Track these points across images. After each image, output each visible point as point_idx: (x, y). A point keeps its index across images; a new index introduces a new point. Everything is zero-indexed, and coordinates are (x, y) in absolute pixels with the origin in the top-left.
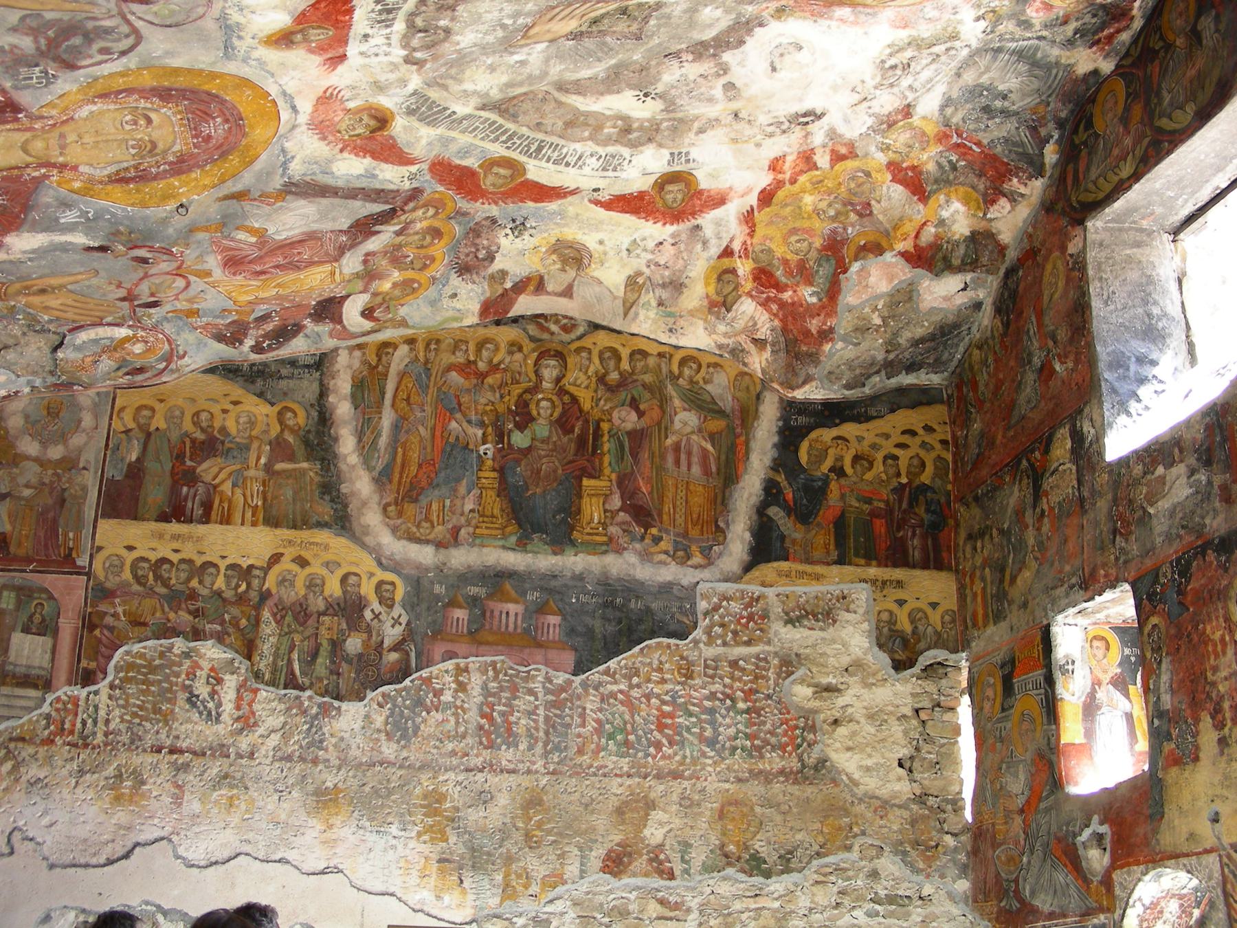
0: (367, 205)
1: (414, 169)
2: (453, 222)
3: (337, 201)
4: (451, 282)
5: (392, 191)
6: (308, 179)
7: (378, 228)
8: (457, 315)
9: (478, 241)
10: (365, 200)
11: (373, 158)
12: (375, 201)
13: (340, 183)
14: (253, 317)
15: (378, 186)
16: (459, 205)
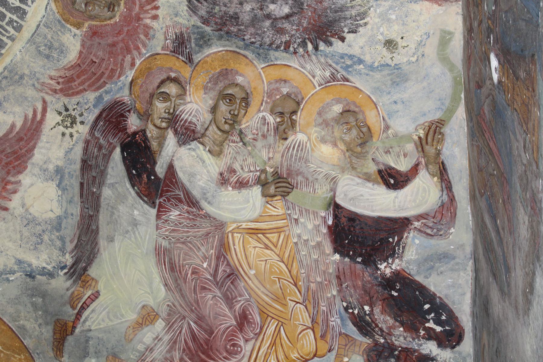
0: (110, 180)
1: (52, 118)
2: (197, 58)
3: (103, 218)
4: (356, 51)
5: (86, 150)
6: (70, 247)
7: (160, 170)
8: (434, 41)
9: (246, 18)
10: (101, 185)
11: (21, 169)
12: (103, 173)
13: (76, 210)
14: (360, 338)
15: (78, 166)
16: (159, 50)
